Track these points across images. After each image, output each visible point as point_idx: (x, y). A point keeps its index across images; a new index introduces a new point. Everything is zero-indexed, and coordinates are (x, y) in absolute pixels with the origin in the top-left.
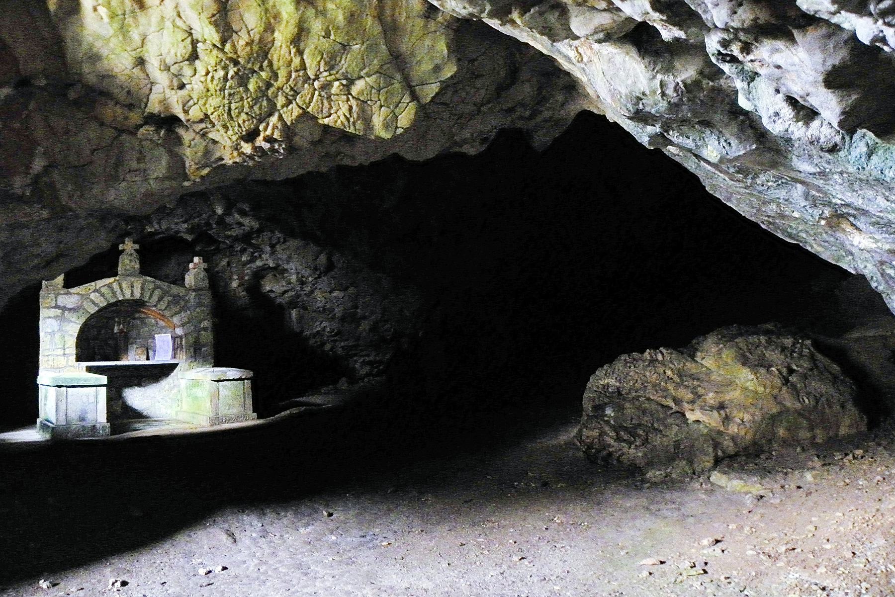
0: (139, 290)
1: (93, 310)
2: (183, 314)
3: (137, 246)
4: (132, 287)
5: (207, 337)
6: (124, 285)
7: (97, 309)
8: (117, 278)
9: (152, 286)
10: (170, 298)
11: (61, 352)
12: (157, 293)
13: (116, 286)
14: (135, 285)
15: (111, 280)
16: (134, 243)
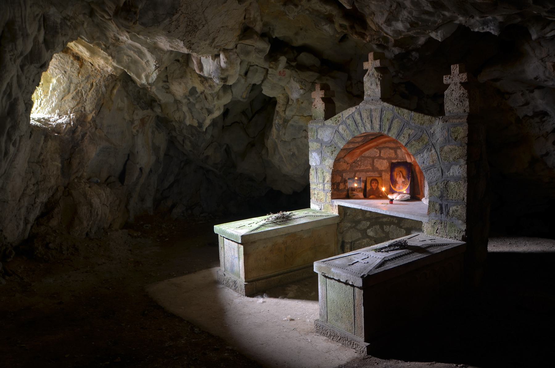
0: (378, 120)
1: (341, 145)
2: (426, 155)
3: (378, 63)
4: (371, 116)
5: (460, 191)
6: (364, 115)
7: (344, 143)
8: (358, 107)
9: (390, 117)
10: (411, 132)
11: (321, 186)
12: (396, 125)
13: (357, 117)
14: (373, 113)
15: (353, 109)
16: (375, 59)
